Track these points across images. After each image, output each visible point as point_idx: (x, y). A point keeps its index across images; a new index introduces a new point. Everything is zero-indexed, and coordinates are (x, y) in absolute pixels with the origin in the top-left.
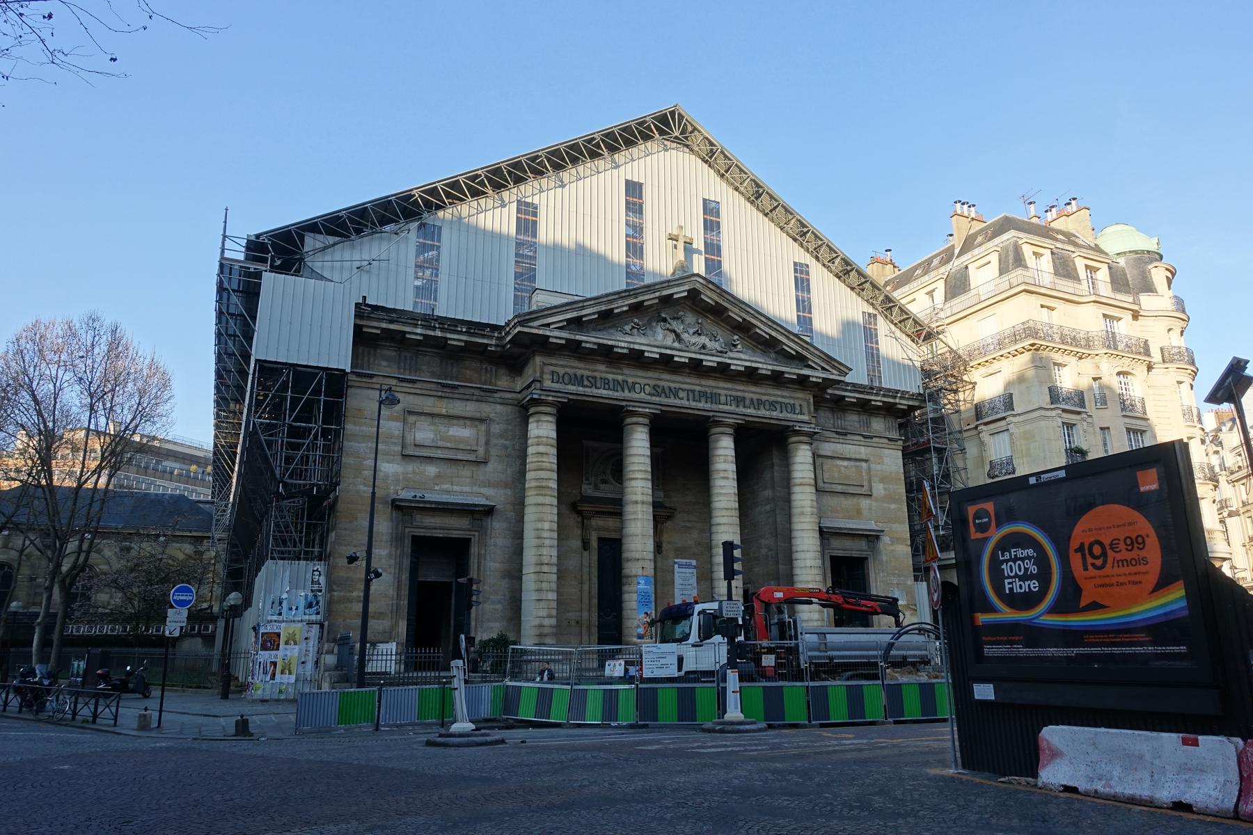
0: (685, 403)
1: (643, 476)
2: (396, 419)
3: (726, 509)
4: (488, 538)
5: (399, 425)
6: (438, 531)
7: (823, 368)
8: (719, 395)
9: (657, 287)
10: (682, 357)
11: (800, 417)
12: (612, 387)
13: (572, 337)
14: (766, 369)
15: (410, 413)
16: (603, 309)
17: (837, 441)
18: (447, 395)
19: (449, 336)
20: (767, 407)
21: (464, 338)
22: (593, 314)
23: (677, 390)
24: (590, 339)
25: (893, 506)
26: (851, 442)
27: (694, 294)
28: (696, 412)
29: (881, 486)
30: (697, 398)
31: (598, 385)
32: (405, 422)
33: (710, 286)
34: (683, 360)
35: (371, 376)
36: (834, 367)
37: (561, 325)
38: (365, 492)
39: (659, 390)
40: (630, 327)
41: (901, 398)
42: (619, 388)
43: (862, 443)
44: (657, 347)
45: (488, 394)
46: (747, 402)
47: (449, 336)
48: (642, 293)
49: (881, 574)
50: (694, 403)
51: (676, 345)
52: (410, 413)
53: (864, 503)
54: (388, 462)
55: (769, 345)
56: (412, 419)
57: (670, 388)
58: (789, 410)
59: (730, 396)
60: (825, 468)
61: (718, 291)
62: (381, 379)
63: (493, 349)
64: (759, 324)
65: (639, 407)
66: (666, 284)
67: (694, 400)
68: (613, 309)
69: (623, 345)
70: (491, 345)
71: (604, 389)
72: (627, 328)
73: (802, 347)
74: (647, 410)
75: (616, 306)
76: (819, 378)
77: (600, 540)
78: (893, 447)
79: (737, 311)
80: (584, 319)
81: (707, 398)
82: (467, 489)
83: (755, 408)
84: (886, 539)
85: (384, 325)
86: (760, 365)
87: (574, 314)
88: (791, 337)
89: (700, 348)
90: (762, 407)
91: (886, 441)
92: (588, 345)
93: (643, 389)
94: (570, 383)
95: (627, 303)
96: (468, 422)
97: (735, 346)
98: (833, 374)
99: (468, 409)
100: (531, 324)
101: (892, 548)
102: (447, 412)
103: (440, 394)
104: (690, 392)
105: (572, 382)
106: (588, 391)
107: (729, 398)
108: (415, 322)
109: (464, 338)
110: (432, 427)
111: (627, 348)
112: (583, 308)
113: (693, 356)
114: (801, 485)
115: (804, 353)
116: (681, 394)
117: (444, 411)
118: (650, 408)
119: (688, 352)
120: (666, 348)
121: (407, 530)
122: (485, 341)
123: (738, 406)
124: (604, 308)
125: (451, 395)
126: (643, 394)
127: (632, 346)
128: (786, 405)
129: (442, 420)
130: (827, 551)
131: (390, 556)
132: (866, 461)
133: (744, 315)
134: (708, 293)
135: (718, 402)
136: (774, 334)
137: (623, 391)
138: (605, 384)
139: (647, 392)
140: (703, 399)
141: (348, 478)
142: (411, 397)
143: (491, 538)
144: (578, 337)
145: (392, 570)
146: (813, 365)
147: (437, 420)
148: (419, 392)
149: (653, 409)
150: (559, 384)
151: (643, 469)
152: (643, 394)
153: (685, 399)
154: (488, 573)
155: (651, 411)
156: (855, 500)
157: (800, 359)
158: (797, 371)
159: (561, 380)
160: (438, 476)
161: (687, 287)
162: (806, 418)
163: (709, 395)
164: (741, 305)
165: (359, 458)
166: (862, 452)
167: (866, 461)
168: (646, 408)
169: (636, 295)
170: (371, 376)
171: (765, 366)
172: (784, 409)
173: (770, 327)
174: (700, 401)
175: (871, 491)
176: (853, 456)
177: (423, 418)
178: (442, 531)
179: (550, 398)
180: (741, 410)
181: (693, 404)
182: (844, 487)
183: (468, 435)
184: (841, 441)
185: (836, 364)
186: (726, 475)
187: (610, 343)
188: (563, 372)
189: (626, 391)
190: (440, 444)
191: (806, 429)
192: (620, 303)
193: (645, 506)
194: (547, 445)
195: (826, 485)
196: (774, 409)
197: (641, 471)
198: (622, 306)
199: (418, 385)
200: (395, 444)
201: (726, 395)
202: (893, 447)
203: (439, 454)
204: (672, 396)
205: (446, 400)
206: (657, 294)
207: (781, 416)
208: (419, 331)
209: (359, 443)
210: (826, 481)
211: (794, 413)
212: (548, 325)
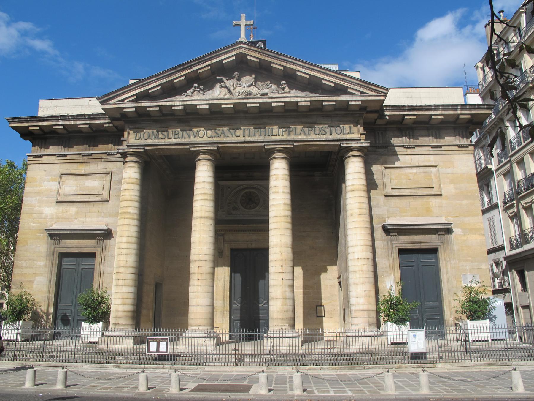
0: (241, 139)
1: (202, 198)
2: (54, 180)
3: (276, 216)
4: (107, 251)
6: (75, 248)
7: (362, 93)
10: (227, 105)
11: (349, 136)
12: (180, 136)
13: (139, 105)
14: (305, 101)
15: (62, 175)
16: (164, 81)
17: (405, 153)
18: (86, 161)
19: (78, 122)
21: (88, 122)
24: (152, 105)
25: (465, 202)
26: (419, 153)
28: (251, 145)
29: (452, 186)
30: (252, 133)
31: (170, 136)
34: (229, 106)
35: (41, 156)
36: (372, 90)
37: (132, 98)
38: (33, 227)
41: (462, 109)
42: (187, 136)
43: (431, 153)
44: (206, 100)
45: (112, 156)
47: (78, 122)
49: (452, 262)
50: (250, 138)
51: (231, 96)
52: (62, 175)
53: (434, 201)
54: (48, 207)
60: (393, 177)
61: (260, 50)
62: (47, 157)
63: (107, 125)
65: (200, 147)
69: (178, 103)
70: (105, 123)
71: (175, 138)
72: (189, 92)
74: (206, 148)
75: (174, 77)
76: (358, 101)
77: (232, 250)
78: (464, 152)
79: (278, 62)
80: (150, 91)
82: (94, 220)
83: (305, 135)
84: (457, 231)
85: (40, 124)
86: (299, 99)
87: (142, 89)
88: (328, 72)
89: (247, 95)
91: (456, 148)
92: (151, 109)
96: (98, 176)
97: (283, 89)
98: (371, 96)
99: (99, 167)
100: (110, 102)
101: (465, 238)
102: (85, 171)
103: (81, 161)
105: (150, 137)
106: (162, 142)
108: (57, 118)
109: (88, 122)
110: (75, 182)
111: (182, 105)
112: (148, 84)
114: (351, 191)
115: (342, 83)
117: (83, 172)
118: (208, 147)
119: (233, 99)
120: (213, 100)
121: (56, 249)
122: (102, 121)
124: (164, 81)
126: (205, 137)
127: (185, 103)
129: (82, 177)
130: (394, 245)
132: (435, 167)
133: (284, 64)
134: (252, 54)
135: (270, 134)
136: (312, 73)
137: (189, 137)
138: (175, 134)
139: (209, 135)
141: (25, 219)
143: (109, 251)
144: (144, 105)
145: (46, 275)
146: (352, 91)
148: (68, 161)
149: (210, 147)
150: (140, 140)
151: (203, 192)
152: (205, 137)
153: (242, 136)
154: (106, 275)
155: (209, 148)
156: (425, 199)
158: (335, 98)
159: (142, 137)
160: (77, 213)
161: (234, 53)
162: (356, 136)
164: (280, 57)
165: (31, 206)
166: (432, 160)
167: (435, 167)
168: (205, 147)
169: (190, 67)
173: (308, 68)
174: (255, 136)
175: (441, 191)
176: (421, 165)
177: (70, 177)
178: (77, 248)
179: (131, 150)
181: (249, 139)
182: (413, 190)
183: (97, 185)
184: (409, 153)
185: (373, 87)
186: (277, 190)
187: (168, 104)
189: (192, 137)
190: (79, 193)
191: (353, 145)
192: (178, 75)
193: (202, 219)
194: (129, 183)
195: (394, 190)
196: (324, 133)
197: (201, 194)
199: (68, 157)
200: (52, 195)
202: (464, 152)
203: (78, 198)
204: (230, 135)
205: (84, 164)
206: (208, 63)
207: (330, 137)
208: (60, 123)
209: (32, 197)
210: (394, 187)
211: (344, 134)
212: (123, 100)
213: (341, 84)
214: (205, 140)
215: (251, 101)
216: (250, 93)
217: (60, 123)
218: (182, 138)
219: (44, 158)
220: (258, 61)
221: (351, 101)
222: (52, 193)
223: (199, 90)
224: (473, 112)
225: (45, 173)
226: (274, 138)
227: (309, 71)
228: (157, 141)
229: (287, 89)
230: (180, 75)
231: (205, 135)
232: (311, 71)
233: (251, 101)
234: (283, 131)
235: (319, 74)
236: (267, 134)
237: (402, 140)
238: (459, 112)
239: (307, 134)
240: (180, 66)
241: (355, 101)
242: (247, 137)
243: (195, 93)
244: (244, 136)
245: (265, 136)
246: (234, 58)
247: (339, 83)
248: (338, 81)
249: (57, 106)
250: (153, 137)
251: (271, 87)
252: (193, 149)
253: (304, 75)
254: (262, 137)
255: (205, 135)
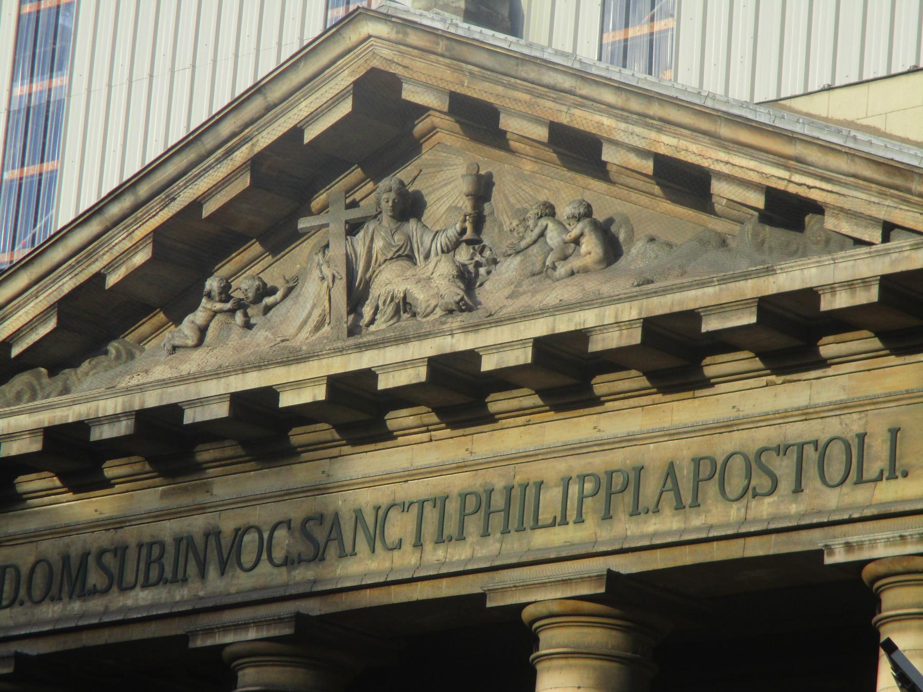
7: (888, 229)
9: (226, 128)
12: (168, 574)
20: (736, 483)
22: (41, 318)
23: (382, 514)
39: (320, 534)
50: (440, 554)
58: (835, 470)
68: (99, 277)
71: (146, 585)
73: (783, 161)
74: (252, 634)
75: (106, 259)
83: (680, 506)
90: (711, 489)
93: (265, 547)
94: (49, 596)
104: (428, 507)
118: (258, 623)
124: (67, 284)
126: (265, 567)
128: (822, 449)
134: (421, 67)
137: (203, 575)
139: (278, 554)
140: (473, 526)
150: (17, 609)
152: (265, 567)
153: (407, 546)
155: (265, 634)
161: (345, 79)
171: (609, 314)
172: (811, 470)
173: (644, 119)
174: (461, 538)
188: (31, 559)
191: (881, 552)
192: (121, 242)
206: (241, 156)
211: (860, 481)
213: (792, 189)
214: (261, 582)
218: (174, 581)
221: (832, 288)
223: (228, 306)
227: (653, 135)
228: (76, 606)
230: (127, 244)
231: (264, 556)
232: (659, 130)
235: (693, 147)
236: (514, 523)
239: (687, 499)
240: (115, 195)
241: (850, 285)
242: (428, 546)
244: (418, 544)
245: (505, 531)
246: (346, 107)
247: (781, 186)
250: (66, 588)
251: (542, 235)
252: (199, 643)
254: (490, 540)
255: (264, 556)
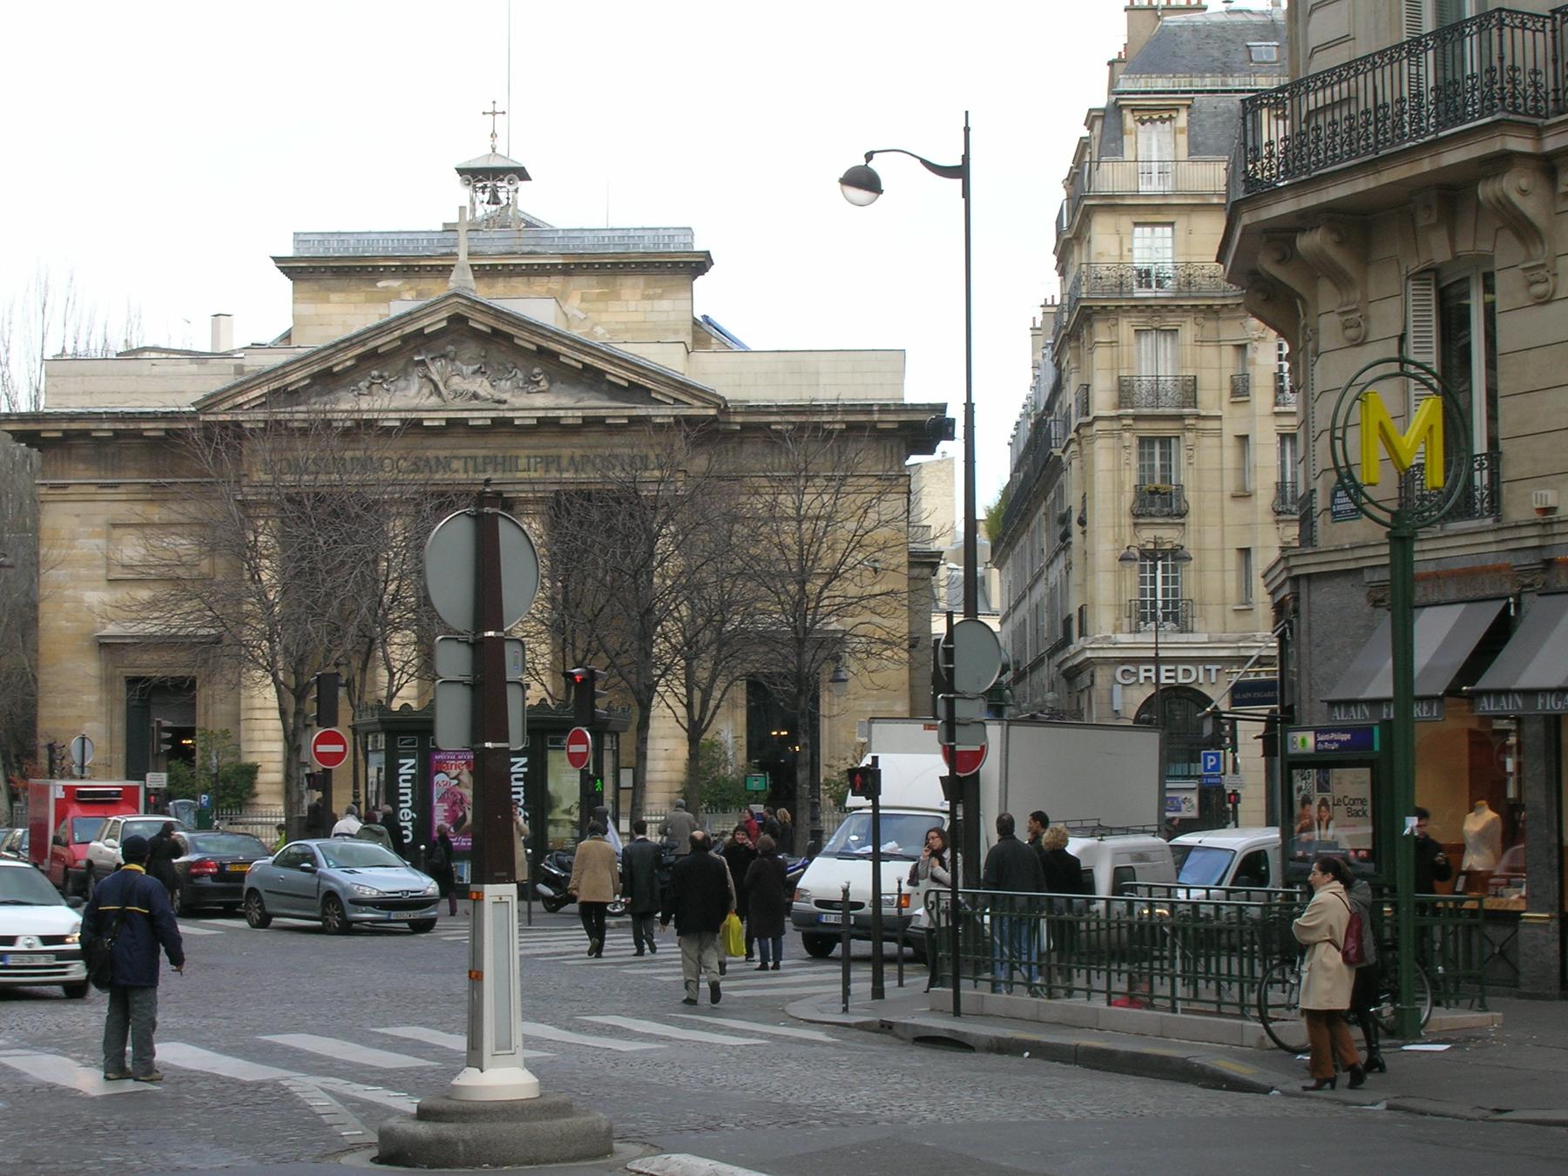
0: (461, 476)
2: (99, 535)
5: (101, 542)
7: (676, 400)
8: (517, 457)
10: (434, 420)
15: (114, 526)
19: (143, 426)
22: (303, 379)
23: (449, 459)
27: (457, 320)
32: (109, 538)
33: (478, 307)
34: (436, 423)
35: (65, 486)
36: (695, 397)
37: (258, 402)
38: (67, 628)
39: (421, 464)
40: (367, 384)
46: (564, 463)
48: (373, 338)
52: (114, 526)
55: (590, 378)
56: (117, 533)
57: (437, 458)
59: (535, 457)
62: (77, 487)
64: (563, 349)
66: (408, 318)
67: (475, 472)
68: (331, 367)
76: (669, 416)
79: (526, 335)
81: (496, 464)
85: (64, 426)
88: (616, 361)
95: (350, 355)
100: (215, 409)
107: (532, 460)
109: (163, 425)
112: (285, 375)
113: (452, 415)
115: (642, 381)
116: (456, 465)
123: (547, 471)
124: (316, 368)
125: (163, 497)
131: (100, 702)
134: (478, 316)
136: (588, 360)
140: (490, 468)
142: (115, 504)
146: (659, 397)
147: (148, 531)
148: (124, 497)
153: (461, 471)
157: (635, 392)
158: (627, 412)
163: (500, 460)
169: (363, 343)
170: (65, 486)
171: (570, 413)
177: (130, 530)
180: (554, 474)
192: (341, 357)
198: (345, 360)
200: (98, 567)
201: (528, 457)
206: (397, 334)
215: (476, 414)
216: (475, 396)
217: (106, 426)
219: (69, 490)
220: (489, 331)
222: (96, 563)
224: (903, 418)
225: (76, 520)
226: (519, 475)
229: (544, 384)
233: (476, 414)
234: (536, 463)
236: (507, 468)
237: (772, 464)
238: (876, 417)
242: (471, 473)
243: (374, 387)
245: (504, 471)
248: (634, 378)
249: (83, 375)
253: (573, 363)
